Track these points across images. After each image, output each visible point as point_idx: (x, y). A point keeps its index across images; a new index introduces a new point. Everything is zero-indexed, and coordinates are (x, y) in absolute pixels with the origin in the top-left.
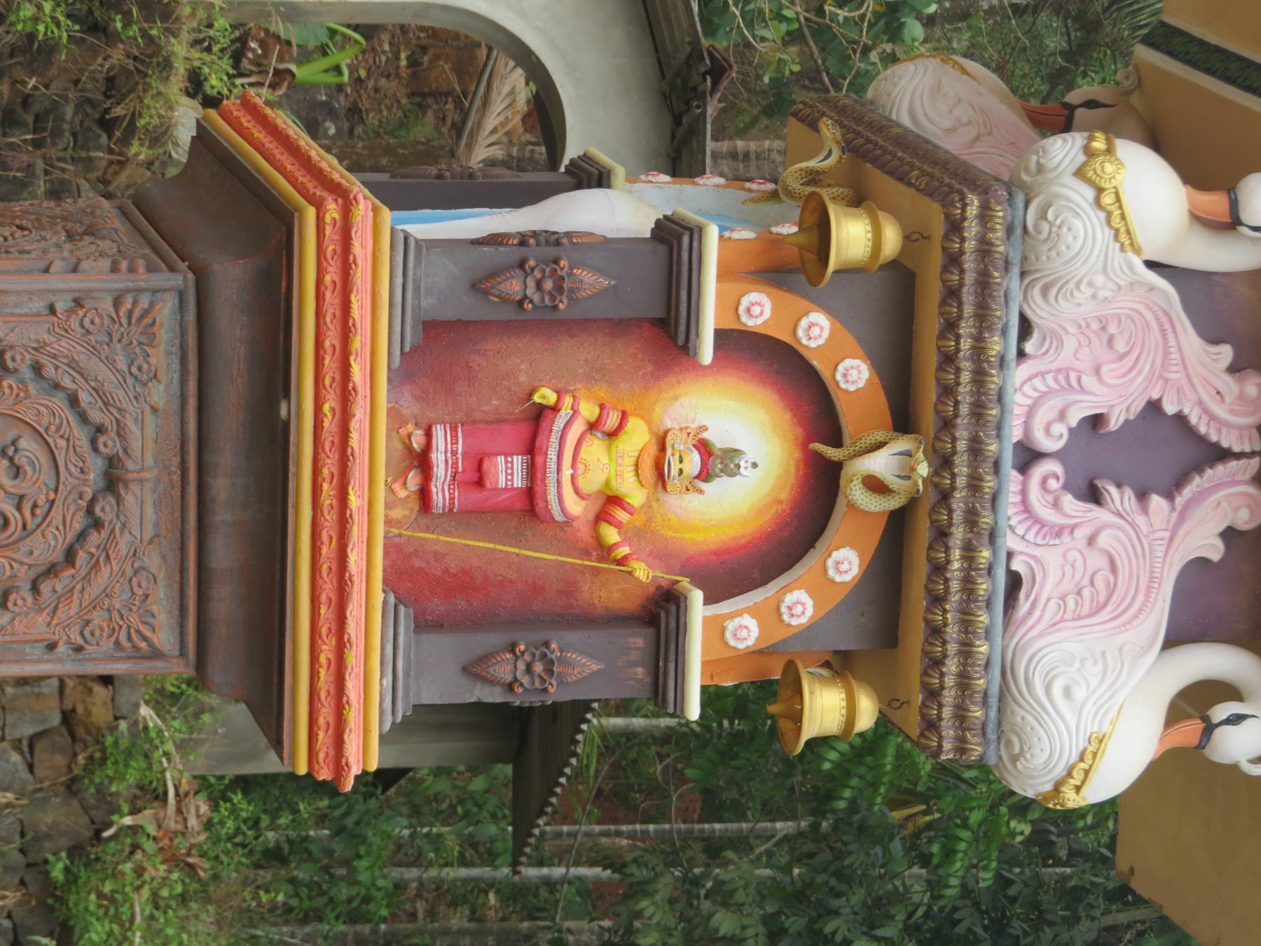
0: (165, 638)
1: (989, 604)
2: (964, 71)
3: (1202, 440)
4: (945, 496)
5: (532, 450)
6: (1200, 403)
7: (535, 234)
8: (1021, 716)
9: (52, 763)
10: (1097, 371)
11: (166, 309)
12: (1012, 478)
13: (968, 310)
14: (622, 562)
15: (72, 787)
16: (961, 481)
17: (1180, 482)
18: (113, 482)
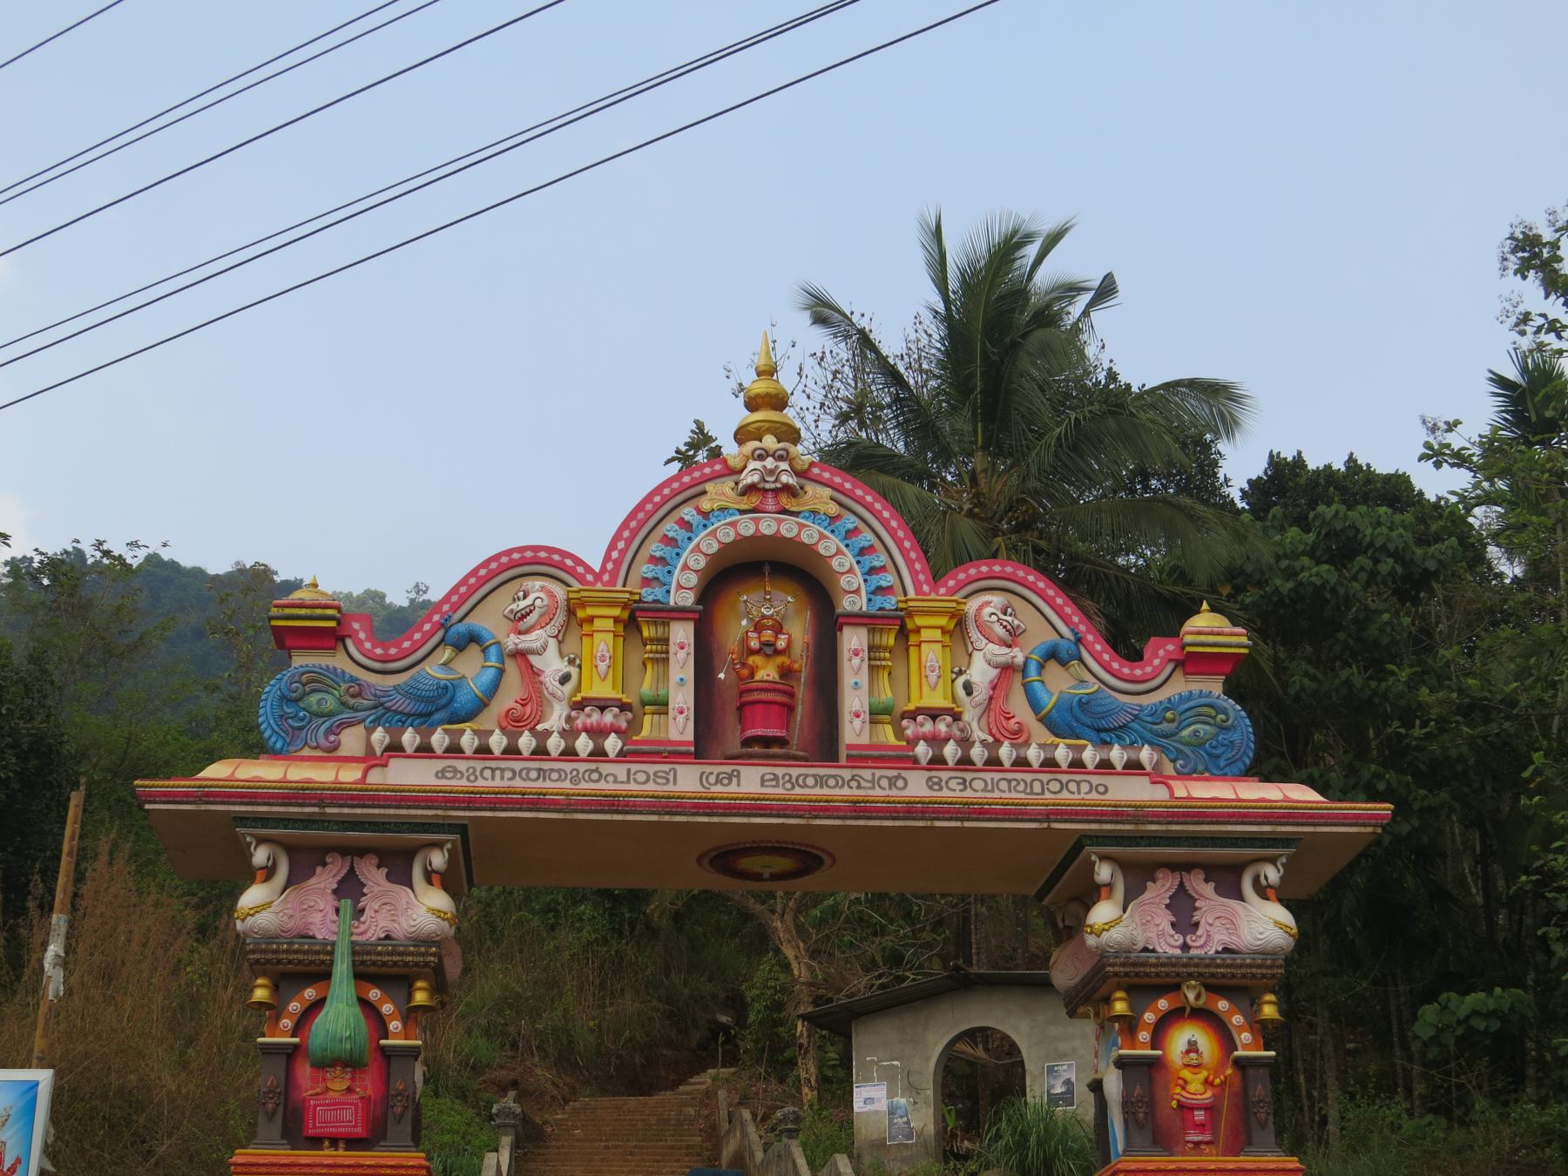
1: (1234, 959)
2: (1055, 962)
3: (1177, 890)
4: (1201, 974)
5: (1192, 1108)
6: (1166, 892)
7: (1123, 1108)
10: (1157, 925)
13: (1142, 969)
14: (1226, 1078)
16: (1196, 970)
17: (1190, 897)
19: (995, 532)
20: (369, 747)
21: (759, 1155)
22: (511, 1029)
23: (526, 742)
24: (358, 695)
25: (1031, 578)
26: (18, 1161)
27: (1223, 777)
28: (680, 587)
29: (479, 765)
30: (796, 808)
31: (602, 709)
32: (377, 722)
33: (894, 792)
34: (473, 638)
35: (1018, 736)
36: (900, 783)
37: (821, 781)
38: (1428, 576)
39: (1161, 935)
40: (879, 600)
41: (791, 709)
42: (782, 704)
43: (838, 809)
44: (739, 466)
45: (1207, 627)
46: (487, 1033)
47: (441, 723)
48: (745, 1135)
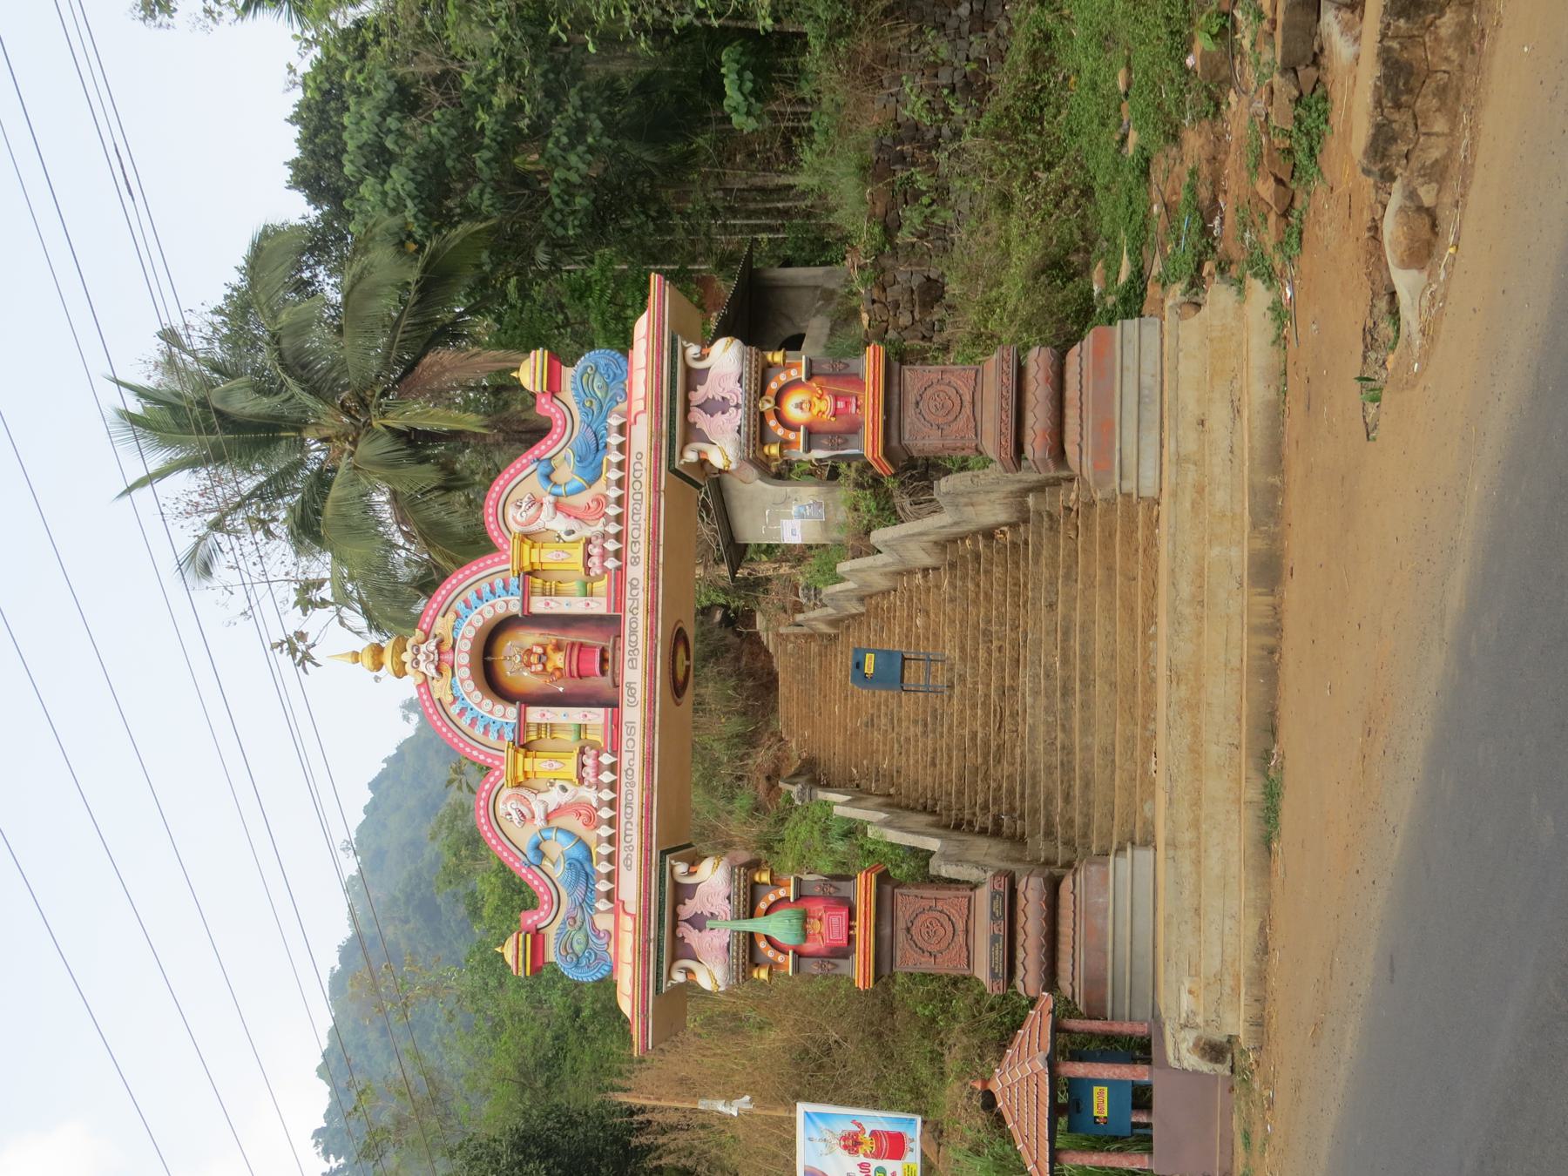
0: (907, 373)
8: (740, 356)
9: (889, 277)
11: (907, 436)
12: (740, 402)
15: (883, 271)
18: (917, 403)
19: (368, 424)
20: (608, 911)
21: (830, 610)
22: (728, 780)
23: (605, 813)
24: (574, 918)
25: (497, 489)
26: (854, 1122)
27: (629, 373)
28: (504, 716)
29: (623, 844)
30: (651, 649)
31: (584, 766)
32: (591, 907)
33: (641, 586)
34: (537, 847)
35: (601, 501)
36: (635, 582)
37: (634, 632)
38: (402, 88)
39: (729, 421)
40: (512, 588)
41: (581, 645)
42: (580, 650)
43: (652, 623)
44: (422, 676)
45: (530, 371)
46: (731, 799)
47: (592, 866)
48: (815, 619)
